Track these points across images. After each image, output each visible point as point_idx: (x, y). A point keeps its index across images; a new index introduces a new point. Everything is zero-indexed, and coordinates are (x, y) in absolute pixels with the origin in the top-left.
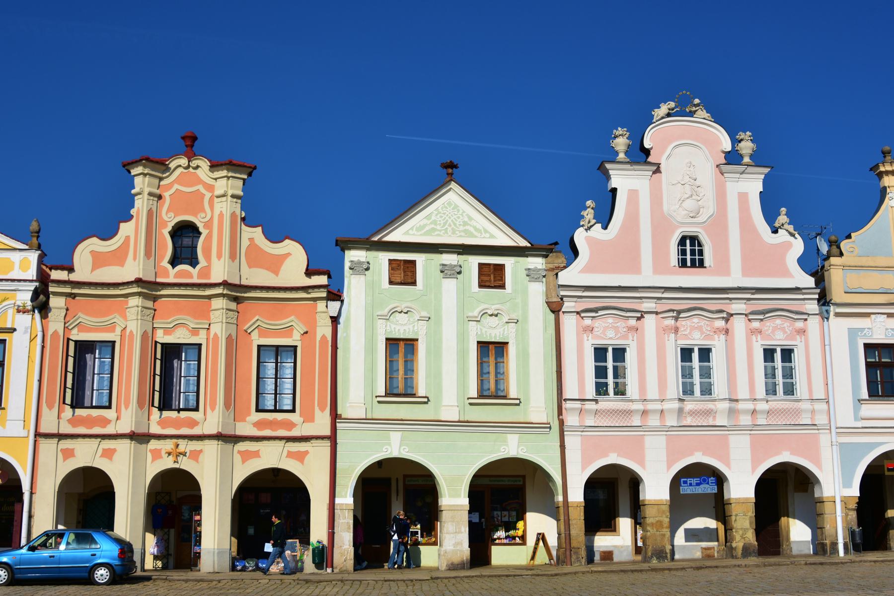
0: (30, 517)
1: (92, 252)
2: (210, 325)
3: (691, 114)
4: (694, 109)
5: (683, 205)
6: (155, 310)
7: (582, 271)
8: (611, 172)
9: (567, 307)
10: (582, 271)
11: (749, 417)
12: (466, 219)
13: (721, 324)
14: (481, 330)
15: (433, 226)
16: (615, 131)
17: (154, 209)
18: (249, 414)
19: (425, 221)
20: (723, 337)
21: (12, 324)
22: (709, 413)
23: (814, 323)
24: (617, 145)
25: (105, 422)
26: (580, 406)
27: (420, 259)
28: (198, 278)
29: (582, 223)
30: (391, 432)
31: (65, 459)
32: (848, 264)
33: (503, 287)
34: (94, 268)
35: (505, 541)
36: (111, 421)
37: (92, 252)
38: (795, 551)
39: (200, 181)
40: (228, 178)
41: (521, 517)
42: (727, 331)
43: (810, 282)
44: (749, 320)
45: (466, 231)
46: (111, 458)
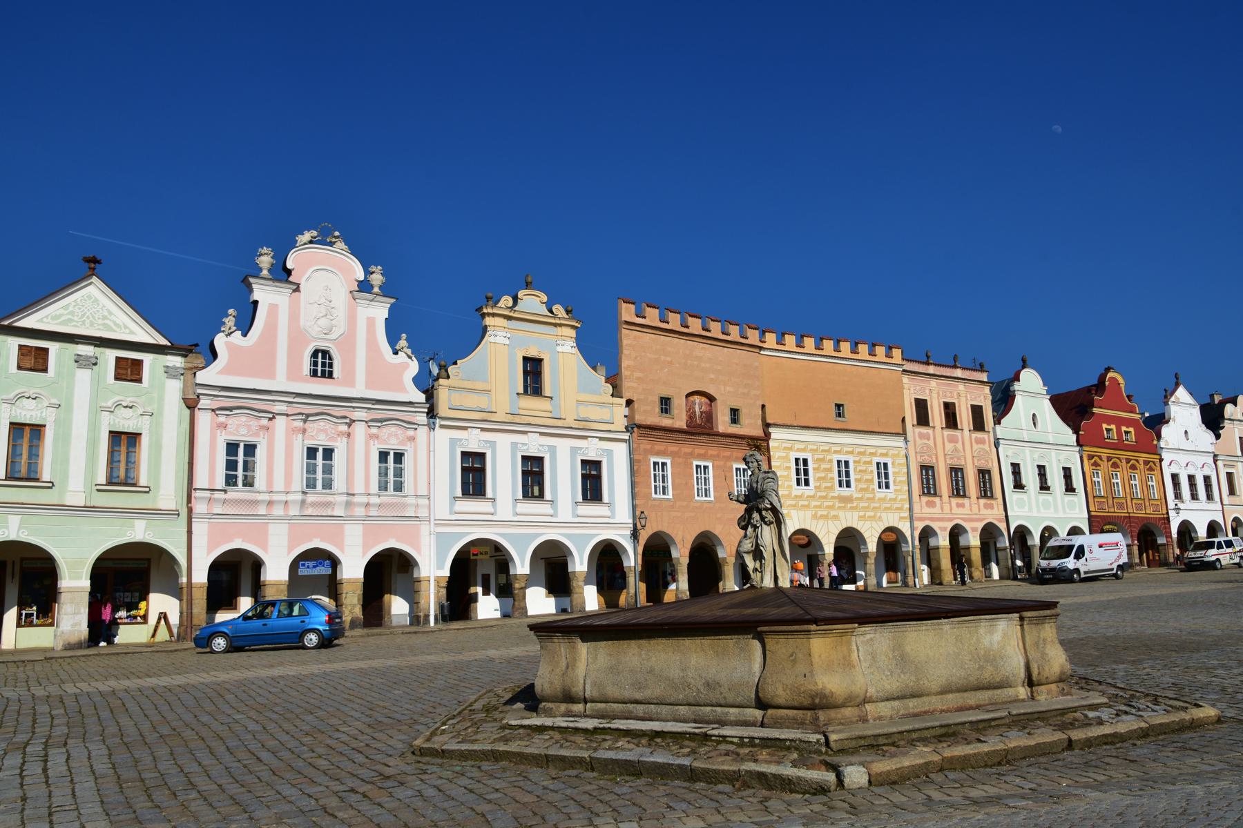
3: (331, 244)
4: (334, 240)
5: (318, 322)
7: (221, 372)
8: (254, 286)
9: (203, 404)
10: (221, 372)
11: (363, 509)
12: (106, 314)
13: (345, 428)
14: (114, 420)
15: (70, 317)
16: (260, 250)
19: (62, 311)
20: (345, 440)
22: (328, 505)
23: (422, 431)
24: (261, 262)
26: (209, 495)
27: (53, 347)
29: (223, 329)
30: (9, 516)
32: (453, 385)
33: (139, 381)
35: (126, 621)
38: (395, 622)
41: (144, 597)
42: (349, 435)
43: (421, 397)
44: (369, 426)
45: (104, 325)
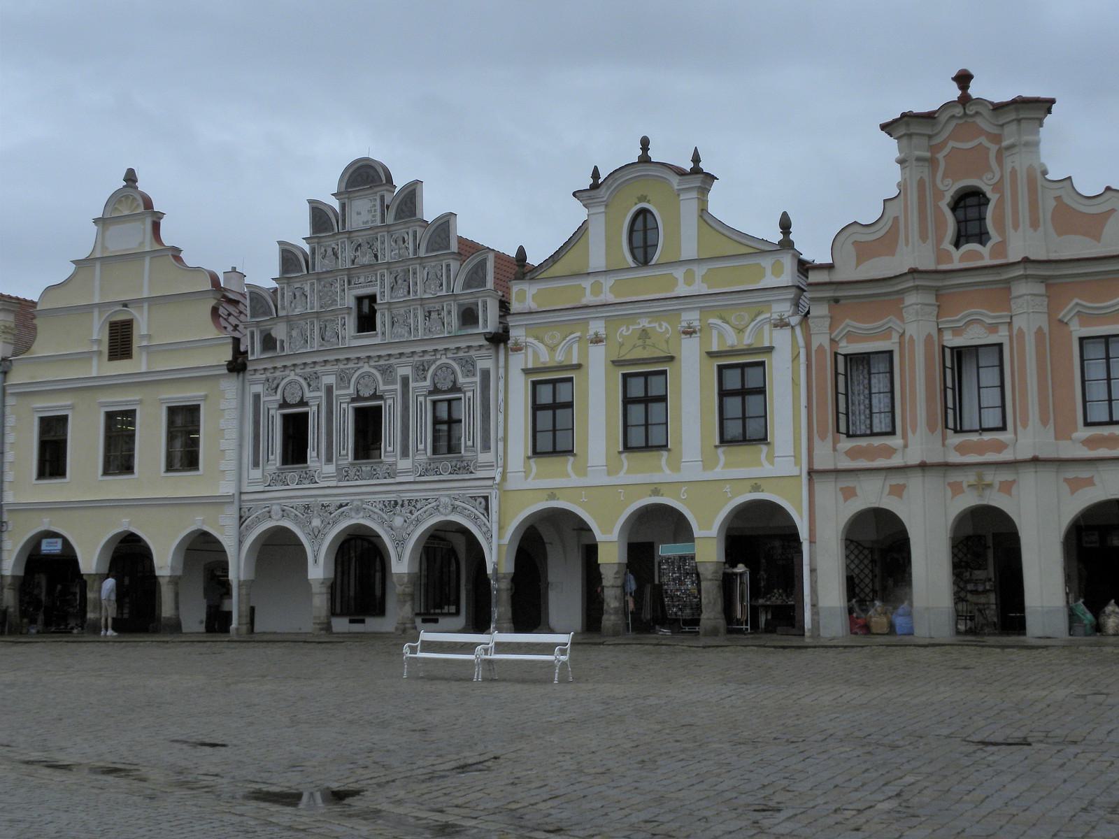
0: (813, 571)
1: (855, 243)
2: (1011, 317)
6: (939, 306)
17: (927, 179)
18: (1076, 430)
21: (771, 341)
25: (890, 451)
28: (991, 259)
31: (846, 499)
34: (860, 261)
36: (896, 450)
37: (855, 243)
39: (982, 132)
40: (1019, 121)
46: (900, 496)
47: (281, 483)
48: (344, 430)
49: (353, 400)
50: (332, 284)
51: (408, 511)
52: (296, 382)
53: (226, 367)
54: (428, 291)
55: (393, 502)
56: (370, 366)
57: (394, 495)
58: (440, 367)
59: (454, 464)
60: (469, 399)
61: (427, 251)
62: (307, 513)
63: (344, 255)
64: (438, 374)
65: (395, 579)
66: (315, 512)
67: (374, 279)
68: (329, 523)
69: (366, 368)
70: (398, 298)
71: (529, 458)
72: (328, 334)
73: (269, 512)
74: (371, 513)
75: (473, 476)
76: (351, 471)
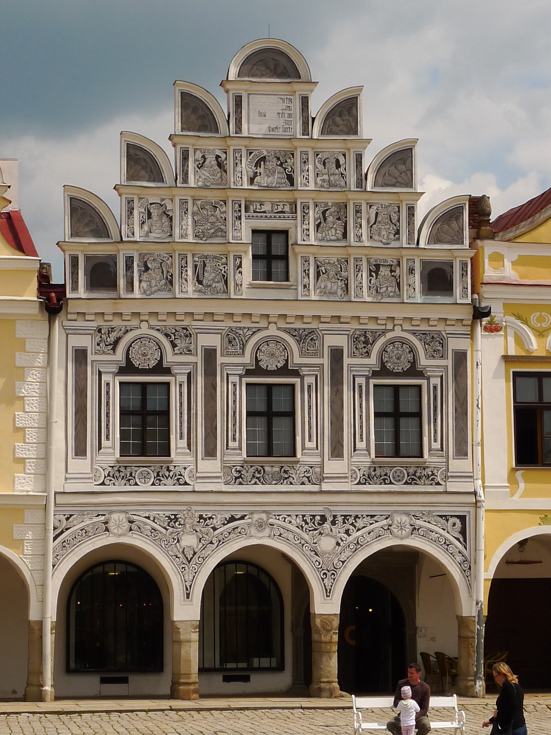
47: (124, 482)
48: (235, 413)
49: (249, 373)
50: (216, 207)
51: (342, 531)
52: (150, 338)
53: (37, 305)
54: (376, 237)
55: (318, 518)
56: (278, 329)
57: (321, 508)
58: (392, 342)
59: (411, 471)
60: (435, 388)
61: (375, 184)
62: (173, 527)
63: (239, 169)
64: (388, 350)
65: (318, 621)
66: (188, 526)
67: (287, 208)
68: (211, 543)
69: (272, 331)
70: (328, 241)
71: (514, 470)
72: (209, 276)
73: (106, 523)
74: (282, 531)
75: (440, 489)
76: (247, 472)
